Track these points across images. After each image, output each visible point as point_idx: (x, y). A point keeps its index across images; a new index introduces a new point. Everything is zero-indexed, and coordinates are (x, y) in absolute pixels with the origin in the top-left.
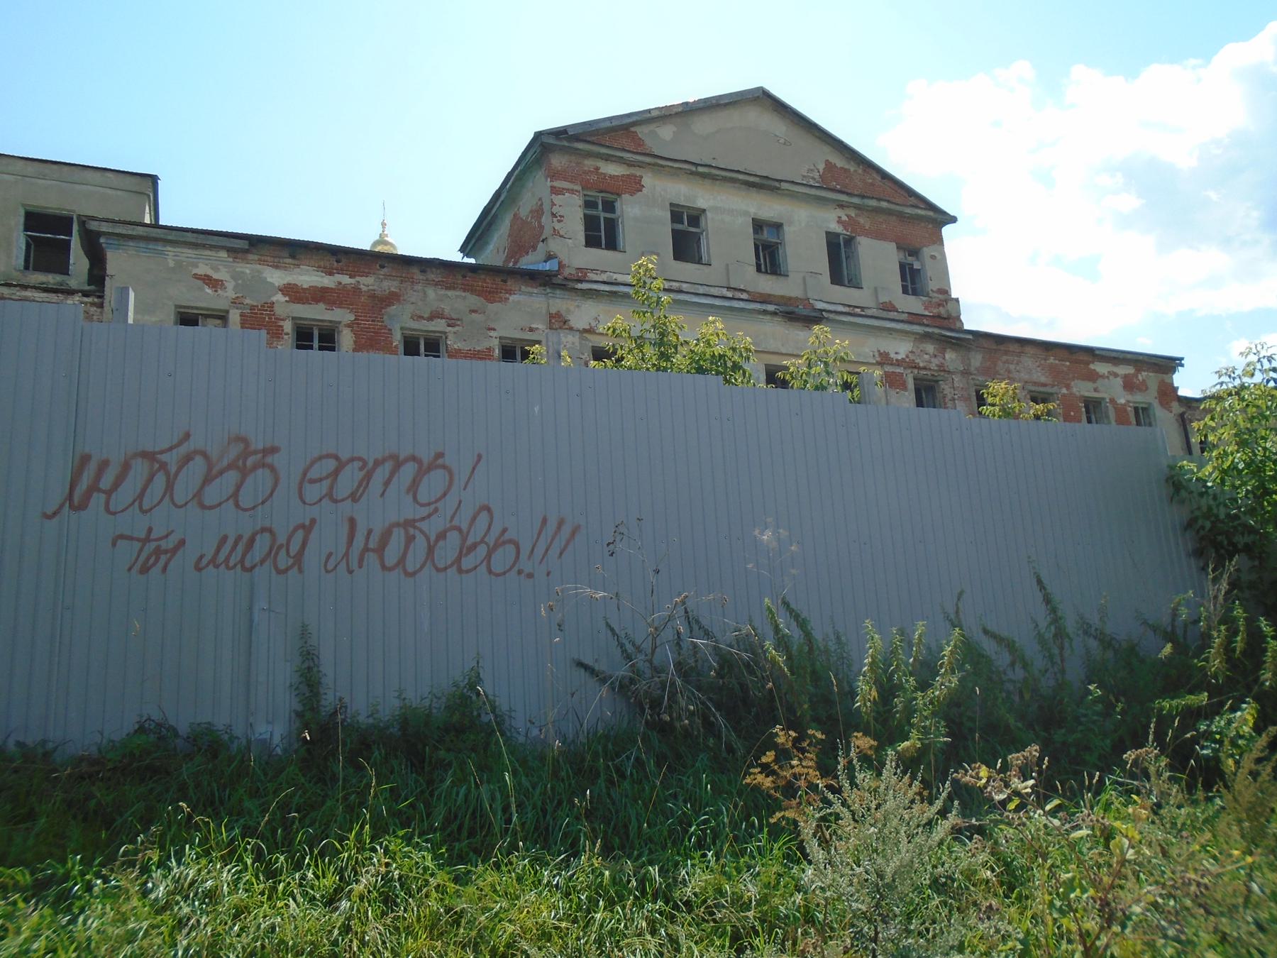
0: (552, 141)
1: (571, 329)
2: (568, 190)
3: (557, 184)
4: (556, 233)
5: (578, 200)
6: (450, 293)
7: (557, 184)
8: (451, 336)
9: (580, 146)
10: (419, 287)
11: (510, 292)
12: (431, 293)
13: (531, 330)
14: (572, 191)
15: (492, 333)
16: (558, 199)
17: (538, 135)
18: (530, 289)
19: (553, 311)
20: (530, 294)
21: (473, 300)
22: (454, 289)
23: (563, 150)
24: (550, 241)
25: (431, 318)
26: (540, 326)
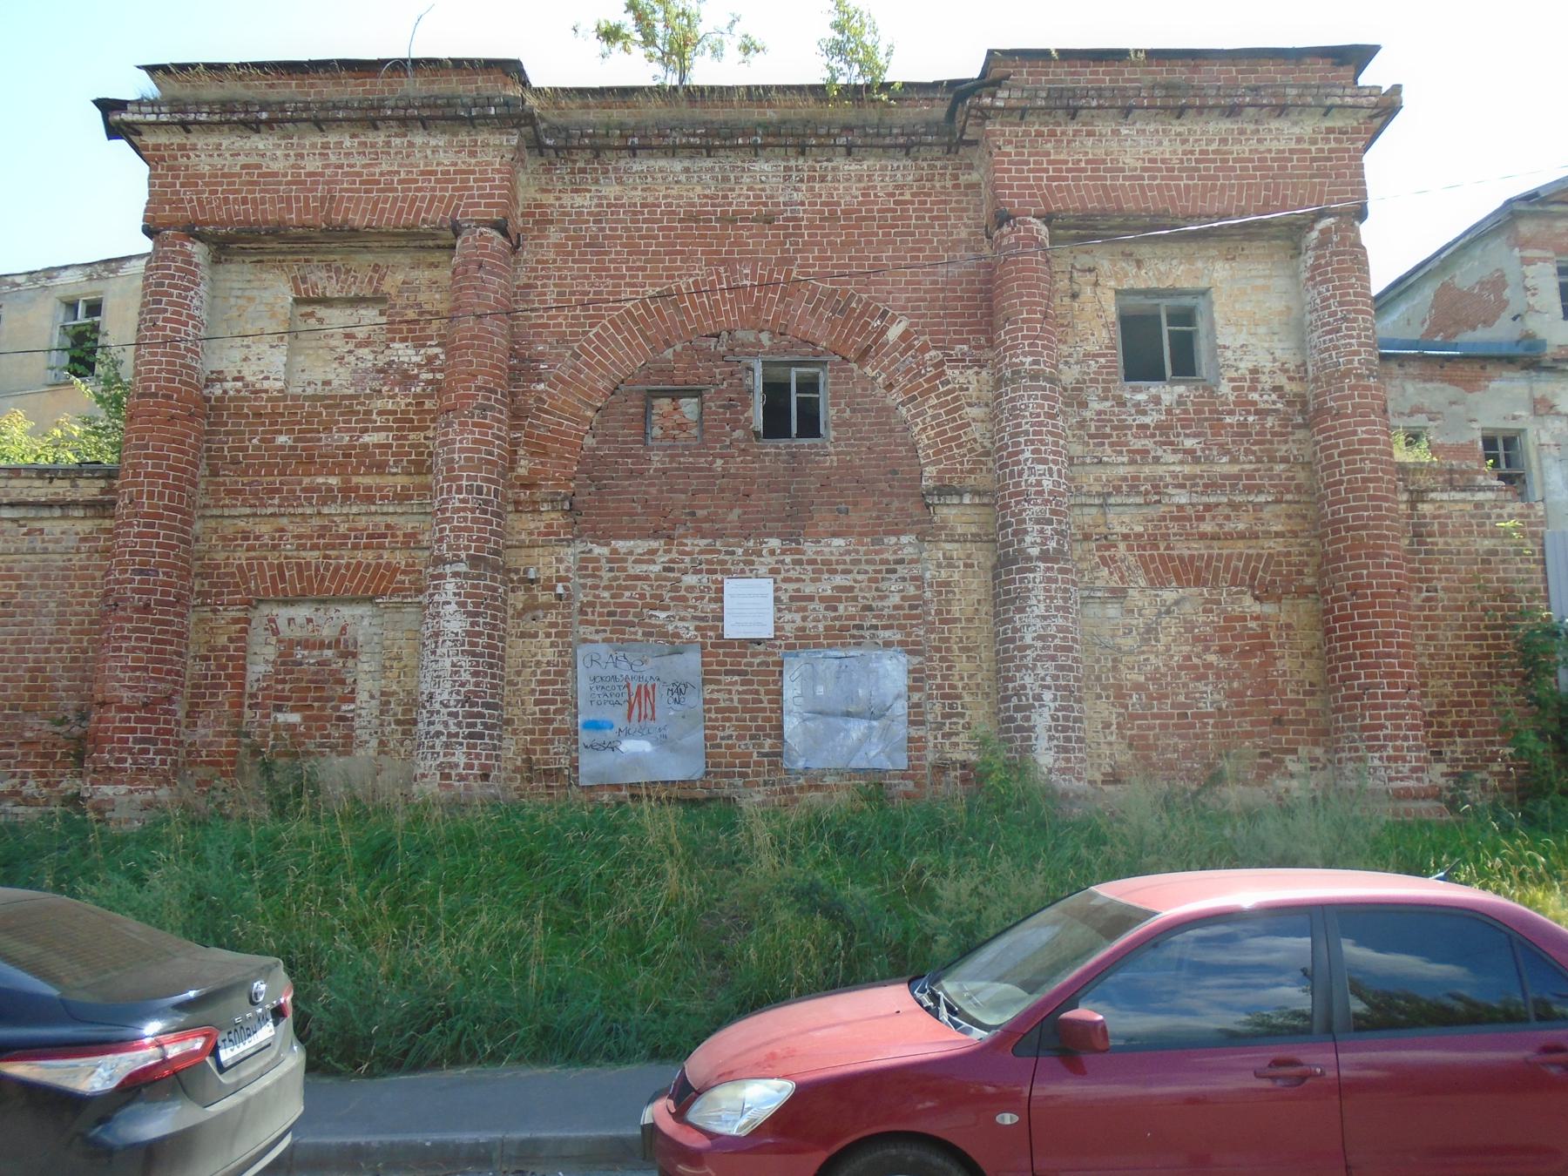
0: (1523, 207)
1: (1558, 414)
2: (1540, 259)
3: (1529, 253)
4: (1530, 308)
5: (1551, 269)
6: (1429, 385)
7: (1529, 253)
8: (1433, 431)
9: (1555, 208)
10: (1397, 382)
11: (1490, 379)
12: (1410, 388)
13: (1514, 418)
14: (1545, 260)
15: (1474, 425)
16: (1530, 270)
17: (1509, 202)
18: (1511, 374)
19: (1538, 395)
20: (1512, 380)
21: (1452, 391)
22: (1431, 380)
23: (1534, 215)
24: (1527, 318)
25: (1411, 414)
26: (1523, 413)
